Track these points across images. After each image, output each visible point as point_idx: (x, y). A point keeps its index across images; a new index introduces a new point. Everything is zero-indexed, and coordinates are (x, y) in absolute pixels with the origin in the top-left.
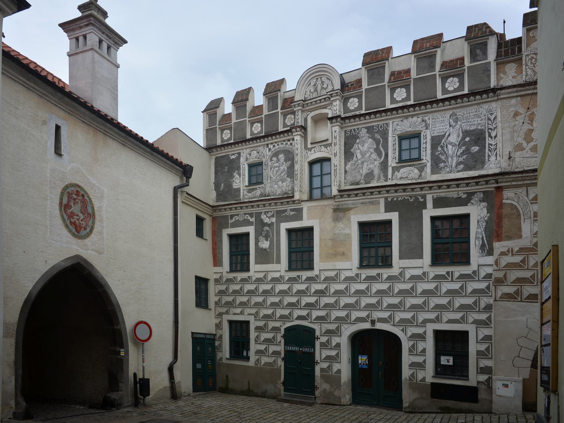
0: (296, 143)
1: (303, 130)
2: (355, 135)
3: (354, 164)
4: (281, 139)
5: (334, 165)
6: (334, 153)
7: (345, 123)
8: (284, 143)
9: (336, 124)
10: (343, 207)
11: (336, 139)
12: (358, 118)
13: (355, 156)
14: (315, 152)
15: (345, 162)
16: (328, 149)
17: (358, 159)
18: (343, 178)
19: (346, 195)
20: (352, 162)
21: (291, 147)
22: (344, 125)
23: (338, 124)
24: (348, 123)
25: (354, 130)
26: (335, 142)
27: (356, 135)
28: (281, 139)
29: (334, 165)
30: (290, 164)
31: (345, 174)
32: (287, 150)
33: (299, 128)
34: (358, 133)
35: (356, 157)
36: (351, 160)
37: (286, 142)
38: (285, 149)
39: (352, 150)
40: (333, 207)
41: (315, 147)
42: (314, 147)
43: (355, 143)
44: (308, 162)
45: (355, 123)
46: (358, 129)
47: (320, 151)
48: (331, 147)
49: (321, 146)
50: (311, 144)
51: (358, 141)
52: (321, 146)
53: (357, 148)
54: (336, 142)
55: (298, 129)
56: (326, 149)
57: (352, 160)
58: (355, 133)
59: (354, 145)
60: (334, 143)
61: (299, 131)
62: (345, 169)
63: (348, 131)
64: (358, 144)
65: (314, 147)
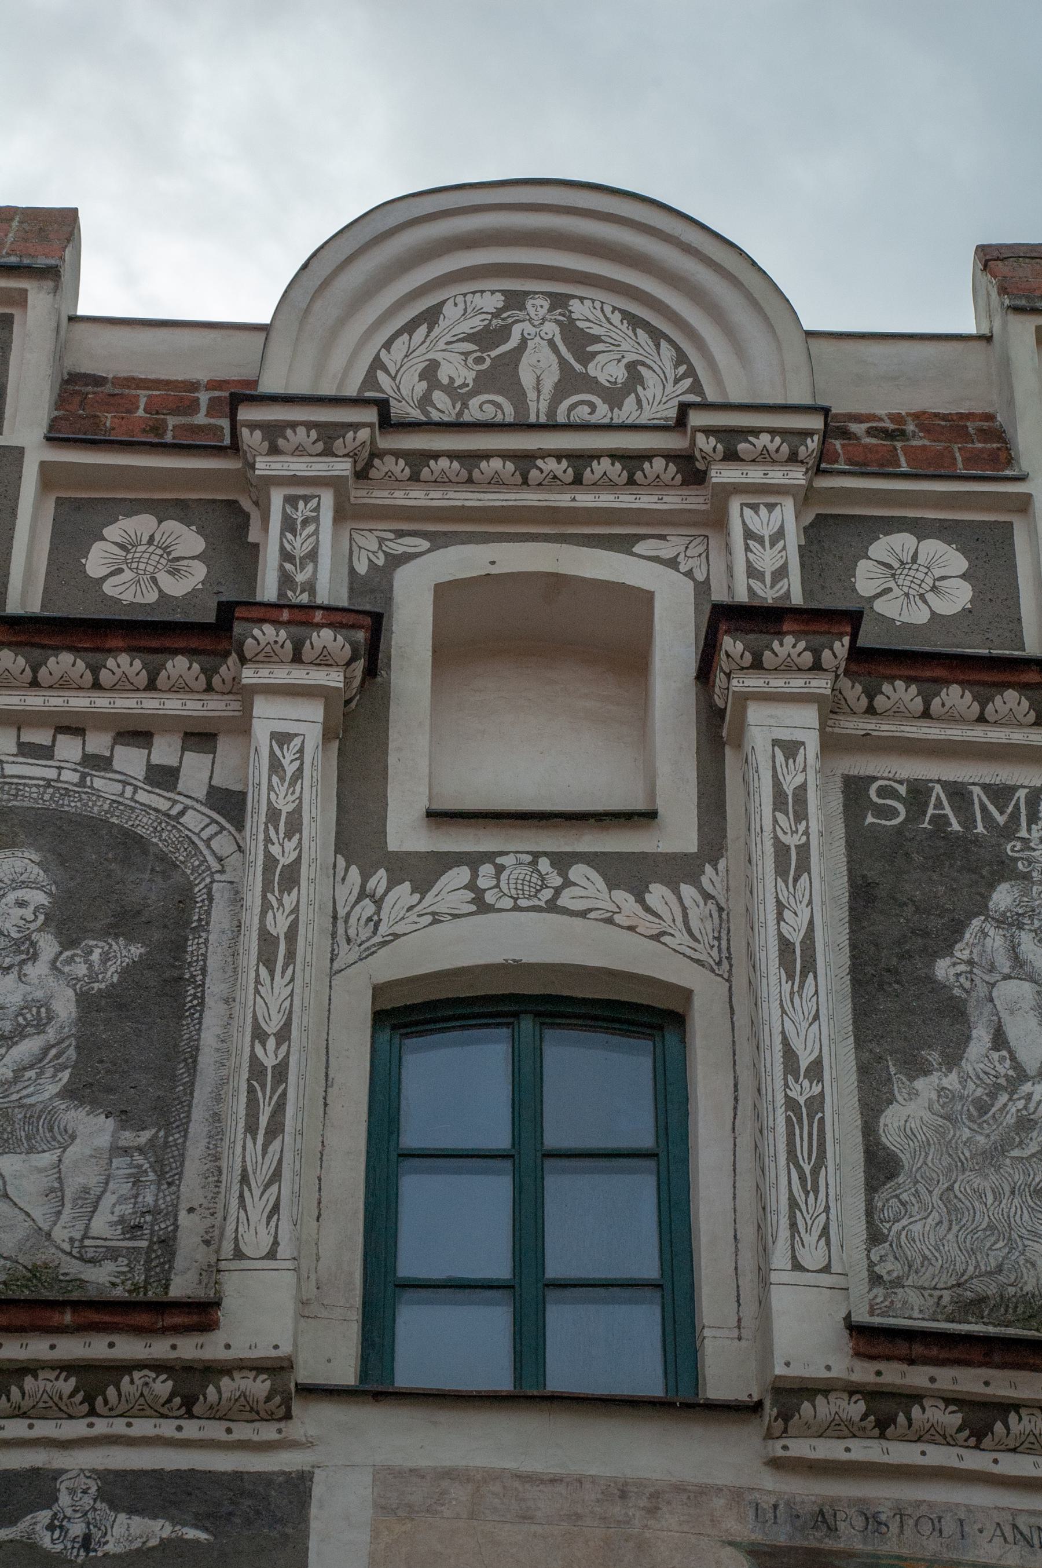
0: (276, 766)
1: (360, 665)
2: (968, 842)
3: (982, 1108)
4: (35, 701)
5: (789, 1053)
6: (785, 946)
7: (871, 710)
8: (69, 749)
9: (797, 684)
10: (890, 1546)
11: (801, 815)
12: (1023, 687)
13: (981, 1037)
14: (483, 907)
15: (864, 1070)
16: (651, 899)
17: (1017, 1066)
18: (859, 1228)
19: (950, 1401)
20: (951, 1081)
21: (163, 805)
22: (854, 726)
23: (821, 685)
24: (897, 713)
25: (958, 793)
26: (792, 841)
27: (976, 840)
28: (35, 701)
29: (789, 1053)
30: (125, 972)
31: (871, 1187)
32: (93, 826)
33: (330, 625)
34: (1009, 831)
35: (999, 1040)
36: (934, 1057)
37: (98, 743)
38: (72, 806)
39: (943, 969)
40: (748, 1531)
41: (489, 857)
42: (474, 861)
43: (982, 908)
44: (378, 990)
45: (977, 734)
46: (1000, 794)
47: (552, 907)
48: (687, 891)
49: (562, 861)
50: (437, 817)
51: (1003, 897)
52: (562, 861)
53: (1004, 965)
54: (804, 850)
55: (325, 638)
56: (624, 898)
57: (952, 1060)
58: (968, 822)
59: (957, 929)
60: (781, 851)
61: (324, 661)
62: (869, 1130)
63: (883, 792)
64: (1011, 922)
65: (474, 861)
